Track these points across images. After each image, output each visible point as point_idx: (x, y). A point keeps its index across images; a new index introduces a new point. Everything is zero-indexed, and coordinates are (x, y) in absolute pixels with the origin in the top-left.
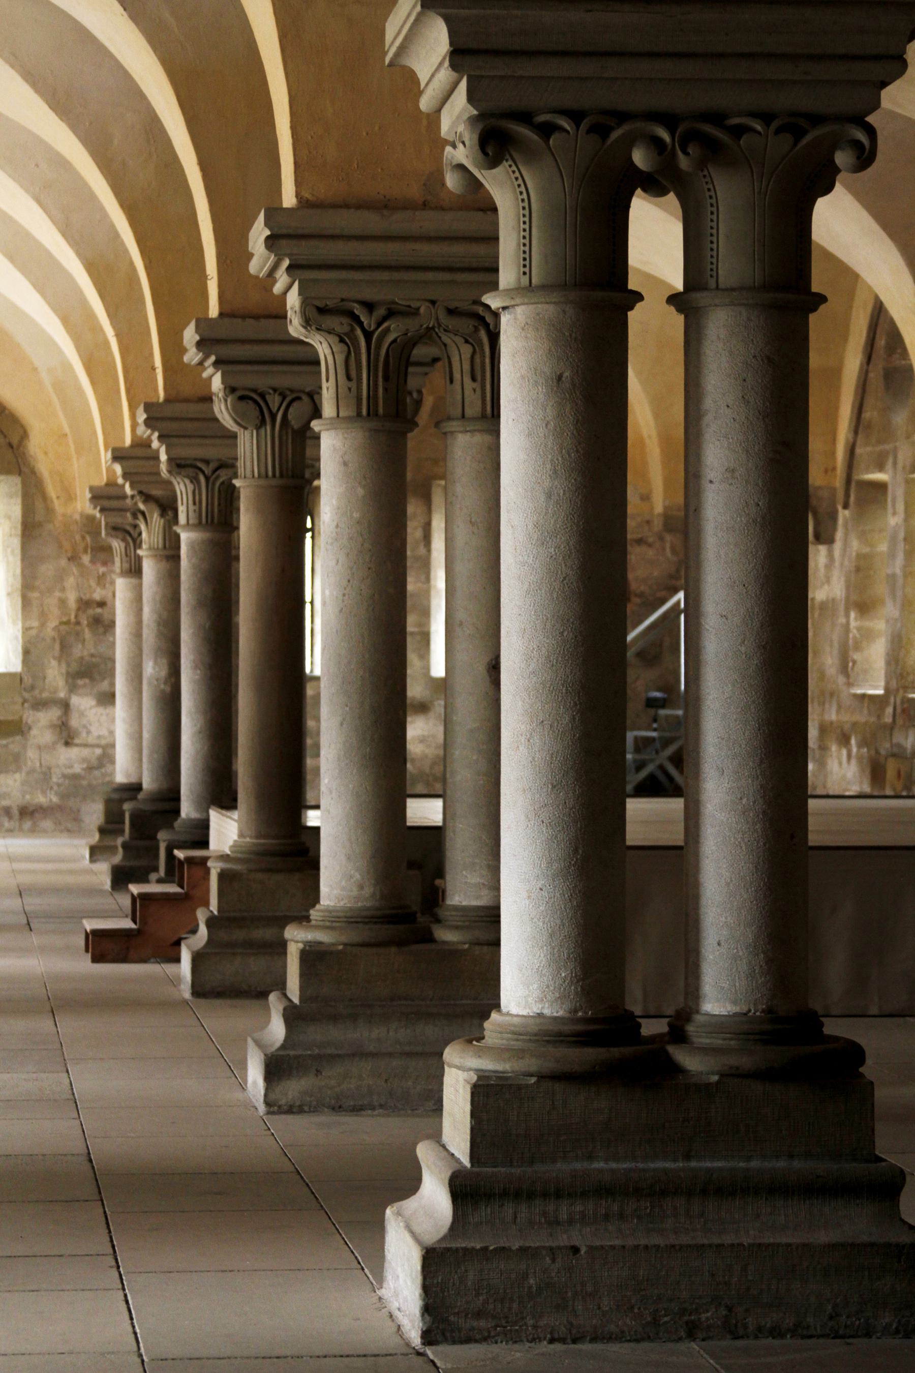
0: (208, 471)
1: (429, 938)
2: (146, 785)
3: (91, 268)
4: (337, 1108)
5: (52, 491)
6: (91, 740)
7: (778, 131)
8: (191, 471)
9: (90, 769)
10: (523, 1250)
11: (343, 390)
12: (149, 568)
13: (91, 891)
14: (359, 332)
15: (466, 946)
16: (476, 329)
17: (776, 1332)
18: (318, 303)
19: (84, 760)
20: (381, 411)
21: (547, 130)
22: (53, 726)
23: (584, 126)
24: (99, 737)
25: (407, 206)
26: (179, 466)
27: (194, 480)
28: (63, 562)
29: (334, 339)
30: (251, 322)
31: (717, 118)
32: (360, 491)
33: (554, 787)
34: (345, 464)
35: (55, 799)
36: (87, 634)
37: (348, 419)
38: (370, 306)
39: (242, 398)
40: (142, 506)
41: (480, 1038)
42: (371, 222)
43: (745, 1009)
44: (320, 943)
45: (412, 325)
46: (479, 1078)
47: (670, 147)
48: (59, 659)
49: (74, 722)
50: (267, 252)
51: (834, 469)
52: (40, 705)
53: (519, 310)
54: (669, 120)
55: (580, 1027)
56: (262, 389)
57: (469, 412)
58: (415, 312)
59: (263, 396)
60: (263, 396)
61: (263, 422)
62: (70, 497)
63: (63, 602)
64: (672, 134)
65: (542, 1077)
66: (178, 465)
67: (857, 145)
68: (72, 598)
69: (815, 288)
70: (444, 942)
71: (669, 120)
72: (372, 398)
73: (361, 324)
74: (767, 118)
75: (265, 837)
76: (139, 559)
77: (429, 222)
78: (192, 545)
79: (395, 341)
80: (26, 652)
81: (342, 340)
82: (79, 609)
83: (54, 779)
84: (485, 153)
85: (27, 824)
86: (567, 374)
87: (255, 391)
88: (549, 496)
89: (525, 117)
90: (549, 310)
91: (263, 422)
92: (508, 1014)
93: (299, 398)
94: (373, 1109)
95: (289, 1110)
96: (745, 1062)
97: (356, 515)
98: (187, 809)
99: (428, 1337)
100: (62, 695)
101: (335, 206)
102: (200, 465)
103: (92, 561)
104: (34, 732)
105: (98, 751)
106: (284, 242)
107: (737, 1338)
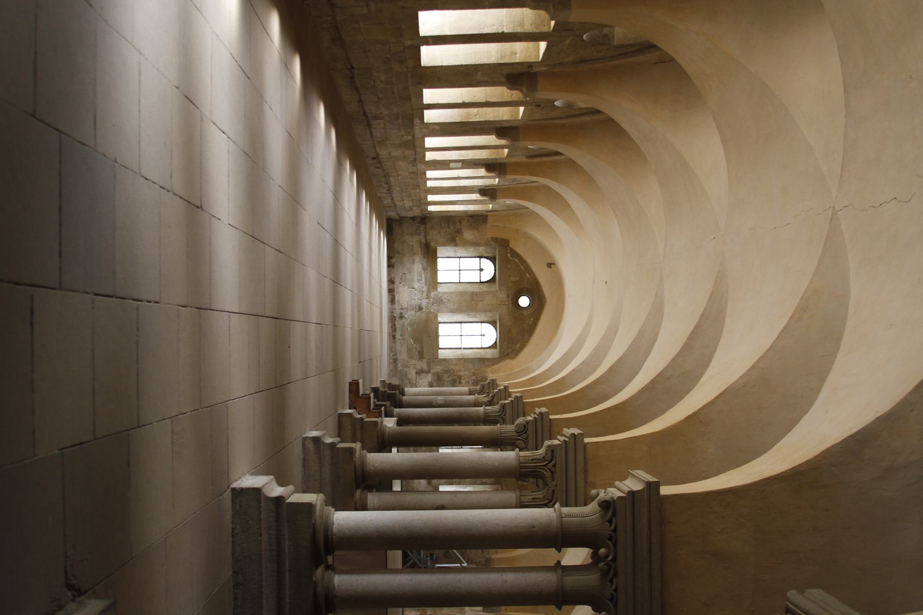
0: (502, 416)
1: (357, 488)
2: (404, 397)
3: (563, 378)
4: (304, 460)
5: (495, 367)
7: (612, 594)
8: (502, 410)
9: (409, 380)
11: (528, 458)
12: (471, 398)
13: (371, 381)
14: (546, 463)
15: (355, 499)
16: (548, 499)
17: (235, 599)
18: (555, 450)
19: (411, 378)
21: (610, 521)
22: (422, 368)
23: (612, 533)
26: (503, 407)
27: (499, 411)
28: (473, 371)
29: (544, 455)
30: (548, 428)
31: (615, 575)
32: (497, 464)
34: (505, 459)
35: (399, 369)
36: (451, 378)
37: (519, 460)
38: (554, 466)
39: (525, 426)
40: (490, 395)
41: (326, 505)
42: (580, 466)
43: (336, 588)
44: (355, 453)
45: (549, 480)
47: (606, 560)
48: (443, 370)
49: (423, 375)
51: (507, 612)
52: (429, 364)
53: (555, 514)
56: (528, 432)
57: (522, 497)
59: (526, 432)
60: (526, 432)
61: (517, 433)
62: (493, 373)
63: (460, 371)
64: (610, 561)
65: (314, 525)
66: (504, 406)
68: (462, 373)
69: (563, 607)
70: (356, 493)
71: (614, 560)
72: (526, 467)
73: (549, 463)
75: (388, 433)
76: (474, 394)
77: (581, 484)
78: (479, 411)
79: (544, 474)
80: (444, 360)
81: (544, 457)
82: (458, 376)
83: (405, 369)
84: (603, 502)
85: (391, 361)
86: (535, 529)
87: (527, 430)
88: (497, 524)
89: (614, 515)
90: (555, 523)
91: (517, 433)
92: (334, 514)
93: (525, 444)
95: (304, 445)
97: (489, 463)
98: (397, 410)
99: (234, 490)
100: (432, 371)
101: (585, 455)
102: (504, 413)
104: (420, 362)
105: (414, 382)
106: (573, 439)
107: (234, 586)
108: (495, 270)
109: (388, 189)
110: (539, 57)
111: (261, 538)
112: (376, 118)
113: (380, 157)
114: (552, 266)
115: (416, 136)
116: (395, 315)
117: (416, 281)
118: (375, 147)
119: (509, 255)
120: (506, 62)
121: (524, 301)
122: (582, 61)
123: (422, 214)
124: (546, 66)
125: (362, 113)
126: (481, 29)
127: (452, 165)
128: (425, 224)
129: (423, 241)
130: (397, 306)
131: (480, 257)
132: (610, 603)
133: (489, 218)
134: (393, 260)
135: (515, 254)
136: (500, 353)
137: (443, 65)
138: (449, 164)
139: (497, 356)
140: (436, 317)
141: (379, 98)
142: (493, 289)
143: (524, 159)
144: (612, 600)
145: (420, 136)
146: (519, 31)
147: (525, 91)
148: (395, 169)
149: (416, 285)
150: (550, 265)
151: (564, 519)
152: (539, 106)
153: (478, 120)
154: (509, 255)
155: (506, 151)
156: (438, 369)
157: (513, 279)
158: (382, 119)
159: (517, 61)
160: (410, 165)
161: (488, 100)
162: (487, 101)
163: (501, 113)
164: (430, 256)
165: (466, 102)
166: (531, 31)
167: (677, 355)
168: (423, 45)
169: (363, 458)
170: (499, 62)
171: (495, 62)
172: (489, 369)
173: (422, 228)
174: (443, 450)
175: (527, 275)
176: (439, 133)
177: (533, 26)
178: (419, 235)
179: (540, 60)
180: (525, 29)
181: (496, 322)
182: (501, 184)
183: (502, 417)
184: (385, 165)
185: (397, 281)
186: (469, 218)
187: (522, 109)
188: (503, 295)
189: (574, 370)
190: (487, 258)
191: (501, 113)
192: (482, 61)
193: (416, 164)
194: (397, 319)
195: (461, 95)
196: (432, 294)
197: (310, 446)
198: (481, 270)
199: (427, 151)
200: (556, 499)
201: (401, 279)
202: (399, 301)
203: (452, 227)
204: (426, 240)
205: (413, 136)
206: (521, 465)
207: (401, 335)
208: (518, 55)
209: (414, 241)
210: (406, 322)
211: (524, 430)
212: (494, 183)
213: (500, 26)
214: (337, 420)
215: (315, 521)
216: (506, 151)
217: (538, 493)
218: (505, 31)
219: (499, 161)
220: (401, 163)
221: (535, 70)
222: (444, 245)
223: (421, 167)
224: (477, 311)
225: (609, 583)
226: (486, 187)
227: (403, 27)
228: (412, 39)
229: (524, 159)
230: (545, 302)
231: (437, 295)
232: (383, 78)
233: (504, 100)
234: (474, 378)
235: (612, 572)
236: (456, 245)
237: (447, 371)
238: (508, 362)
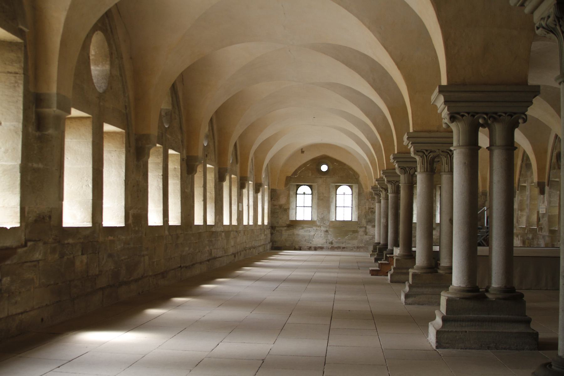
1: (437, 272)
3: (372, 145)
4: (419, 304)
5: (364, 187)
6: (370, 234)
7: (508, 116)
8: (391, 183)
10: (456, 331)
12: (382, 201)
14: (425, 156)
15: (444, 274)
16: (447, 155)
17: (505, 349)
18: (417, 150)
19: (369, 238)
20: (429, 170)
21: (463, 116)
23: (470, 115)
24: (372, 234)
25: (434, 131)
26: (389, 182)
27: (392, 184)
28: (366, 200)
30: (403, 154)
31: (496, 113)
32: (425, 186)
33: (463, 242)
34: (422, 180)
35: (363, 245)
36: (370, 214)
37: (422, 172)
38: (427, 151)
39: (401, 169)
40: (381, 190)
42: (427, 135)
43: (500, 286)
45: (435, 154)
46: (448, 298)
48: (364, 219)
49: (367, 231)
50: (407, 141)
52: (361, 227)
53: (457, 150)
54: (486, 114)
55: (468, 289)
56: (405, 167)
57: (446, 171)
58: (435, 152)
59: (405, 168)
61: (405, 173)
62: (367, 188)
63: (365, 208)
65: (460, 298)
66: (389, 182)
67: (523, 118)
68: (367, 207)
70: (440, 273)
71: (486, 114)
72: (427, 168)
73: (425, 154)
74: (506, 113)
77: (439, 135)
79: (431, 157)
80: (358, 217)
81: (421, 157)
82: (368, 209)
85: (358, 250)
86: (466, 162)
87: (403, 167)
89: (458, 113)
90: (463, 150)
92: (454, 286)
94: (425, 304)
95: (409, 304)
96: (500, 296)
97: (424, 190)
98: (389, 247)
99: (437, 347)
100: (365, 225)
102: (393, 182)
103: (371, 200)
104: (360, 232)
105: (372, 236)
106: (410, 139)
107: (497, 350)
108: (305, 185)
109: (253, 249)
110: (178, 154)
111: (468, 332)
112: (211, 254)
113: (234, 252)
114: (303, 150)
115: (222, 231)
116: (330, 247)
117: (310, 234)
118: (228, 256)
119: (296, 176)
120: (180, 174)
121: (324, 168)
122: (181, 128)
123: (269, 228)
124: (183, 151)
125: (207, 262)
126: (160, 188)
127: (240, 209)
128: (275, 227)
129: (286, 228)
130: (325, 246)
131: (297, 194)
132: (513, 118)
133: (272, 188)
134: (297, 247)
135: (295, 173)
136: (355, 183)
137: (180, 212)
138: (240, 211)
139: (357, 185)
140: (332, 221)
141: (199, 252)
142: (316, 187)
143: (238, 165)
144: (512, 116)
147: (197, 163)
149: (312, 233)
150: (303, 152)
151: (460, 145)
152: (207, 155)
153: (214, 192)
154: (296, 176)
155: (233, 176)
156: (364, 222)
157: (310, 175)
158: (212, 251)
159: (180, 167)
160: (240, 234)
161: (202, 186)
162: (203, 187)
163: (211, 178)
164: (295, 224)
166: (162, 158)
167: (360, 74)
168: (168, 224)
169: (419, 268)
170: (180, 178)
171: (180, 180)
172: (365, 190)
173: (278, 229)
174: (415, 220)
175: (308, 166)
176: (221, 216)
177: (159, 157)
178: (282, 230)
179: (179, 154)
180: (161, 162)
181: (336, 185)
182: (253, 180)
183: (395, 183)
184: (239, 249)
185: (309, 245)
186: (272, 200)
187: (208, 166)
188: (320, 181)
189: (368, 139)
190: (297, 190)
191: (211, 178)
192: (179, 189)
193: (239, 230)
194: (333, 246)
195: (199, 202)
196: (318, 224)
197: (410, 300)
198: (304, 194)
199: (232, 224)
200: (447, 150)
201: (308, 242)
202: (322, 244)
203: (278, 211)
204: (285, 226)
205: (222, 232)
206: (425, 171)
207: (343, 243)
208: (176, 167)
209: (285, 234)
210: (335, 240)
211: (404, 169)
212: (252, 184)
213: (159, 177)
214: (394, 284)
215: (458, 298)
216: (233, 176)
217: (443, 161)
218: (161, 174)
220: (238, 240)
221: (185, 157)
222: (288, 216)
223: (241, 228)
224: (329, 197)
225: (501, 117)
226: (254, 189)
227: (157, 235)
229: (238, 165)
230: (323, 155)
231: (319, 221)
233: (203, 176)
234: (370, 200)
235: (494, 115)
236: (289, 209)
237: (366, 216)
238: (361, 179)
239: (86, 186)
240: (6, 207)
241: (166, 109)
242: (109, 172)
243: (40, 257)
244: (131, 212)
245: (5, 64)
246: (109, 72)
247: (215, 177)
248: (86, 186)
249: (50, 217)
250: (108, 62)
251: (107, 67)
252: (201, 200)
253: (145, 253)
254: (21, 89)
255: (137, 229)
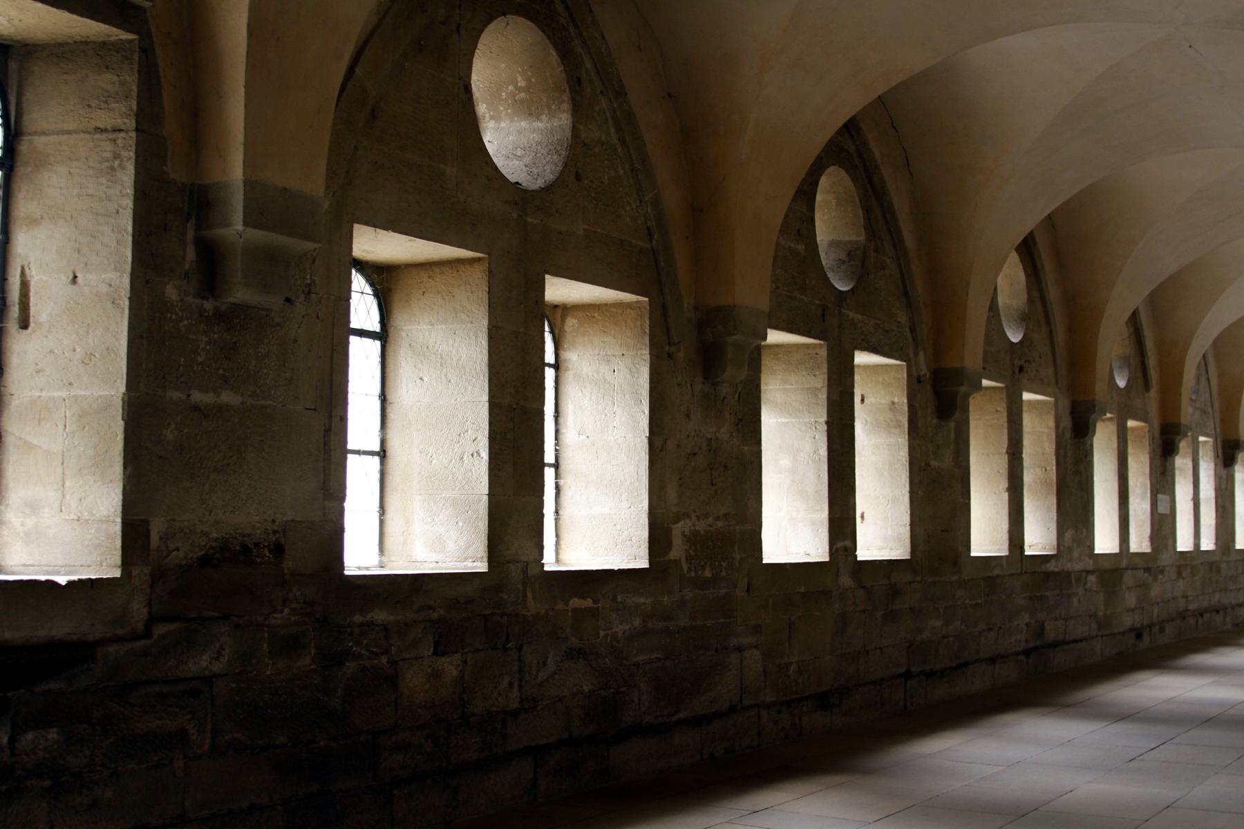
109: (1214, 614)
110: (899, 365)
112: (1041, 632)
113: (1139, 625)
115: (1091, 568)
118: (1113, 635)
120: (906, 419)
122: (906, 294)
124: (916, 354)
125: (1022, 658)
126: (820, 459)
127: (1163, 508)
137: (908, 524)
138: (1160, 514)
141: (990, 629)
143: (1153, 393)
145: (1091, 561)
146: (825, 396)
147: (963, 389)
148: (1169, 600)
153: (1054, 468)
159: (906, 401)
160: (1161, 577)
161: (1004, 451)
162: (1007, 453)
165: (1007, 485)
166: (826, 376)
170: (906, 430)
176: (1084, 531)
177: (817, 373)
179: (904, 363)
180: (822, 387)
182: (1213, 432)
184: (1158, 617)
192: (904, 459)
193: (1159, 567)
195: (995, 493)
199: (1128, 548)
205: (1088, 572)
212: (1211, 444)
213: (816, 428)
218: (824, 418)
219: (1157, 434)
220: (1155, 591)
221: (924, 370)
223: (1165, 559)
226: (1218, 456)
227: (802, 589)
228: (837, 574)
229: (1153, 393)
232: (938, 623)
233: (1006, 424)
239: (472, 455)
240: (87, 521)
241: (850, 242)
242: (606, 415)
243: (217, 667)
244: (678, 531)
245: (89, 106)
246: (568, 133)
247: (1057, 427)
248: (472, 455)
249: (278, 549)
250: (566, 106)
251: (564, 120)
252: (1001, 487)
253: (746, 640)
254: (127, 177)
255: (708, 573)
